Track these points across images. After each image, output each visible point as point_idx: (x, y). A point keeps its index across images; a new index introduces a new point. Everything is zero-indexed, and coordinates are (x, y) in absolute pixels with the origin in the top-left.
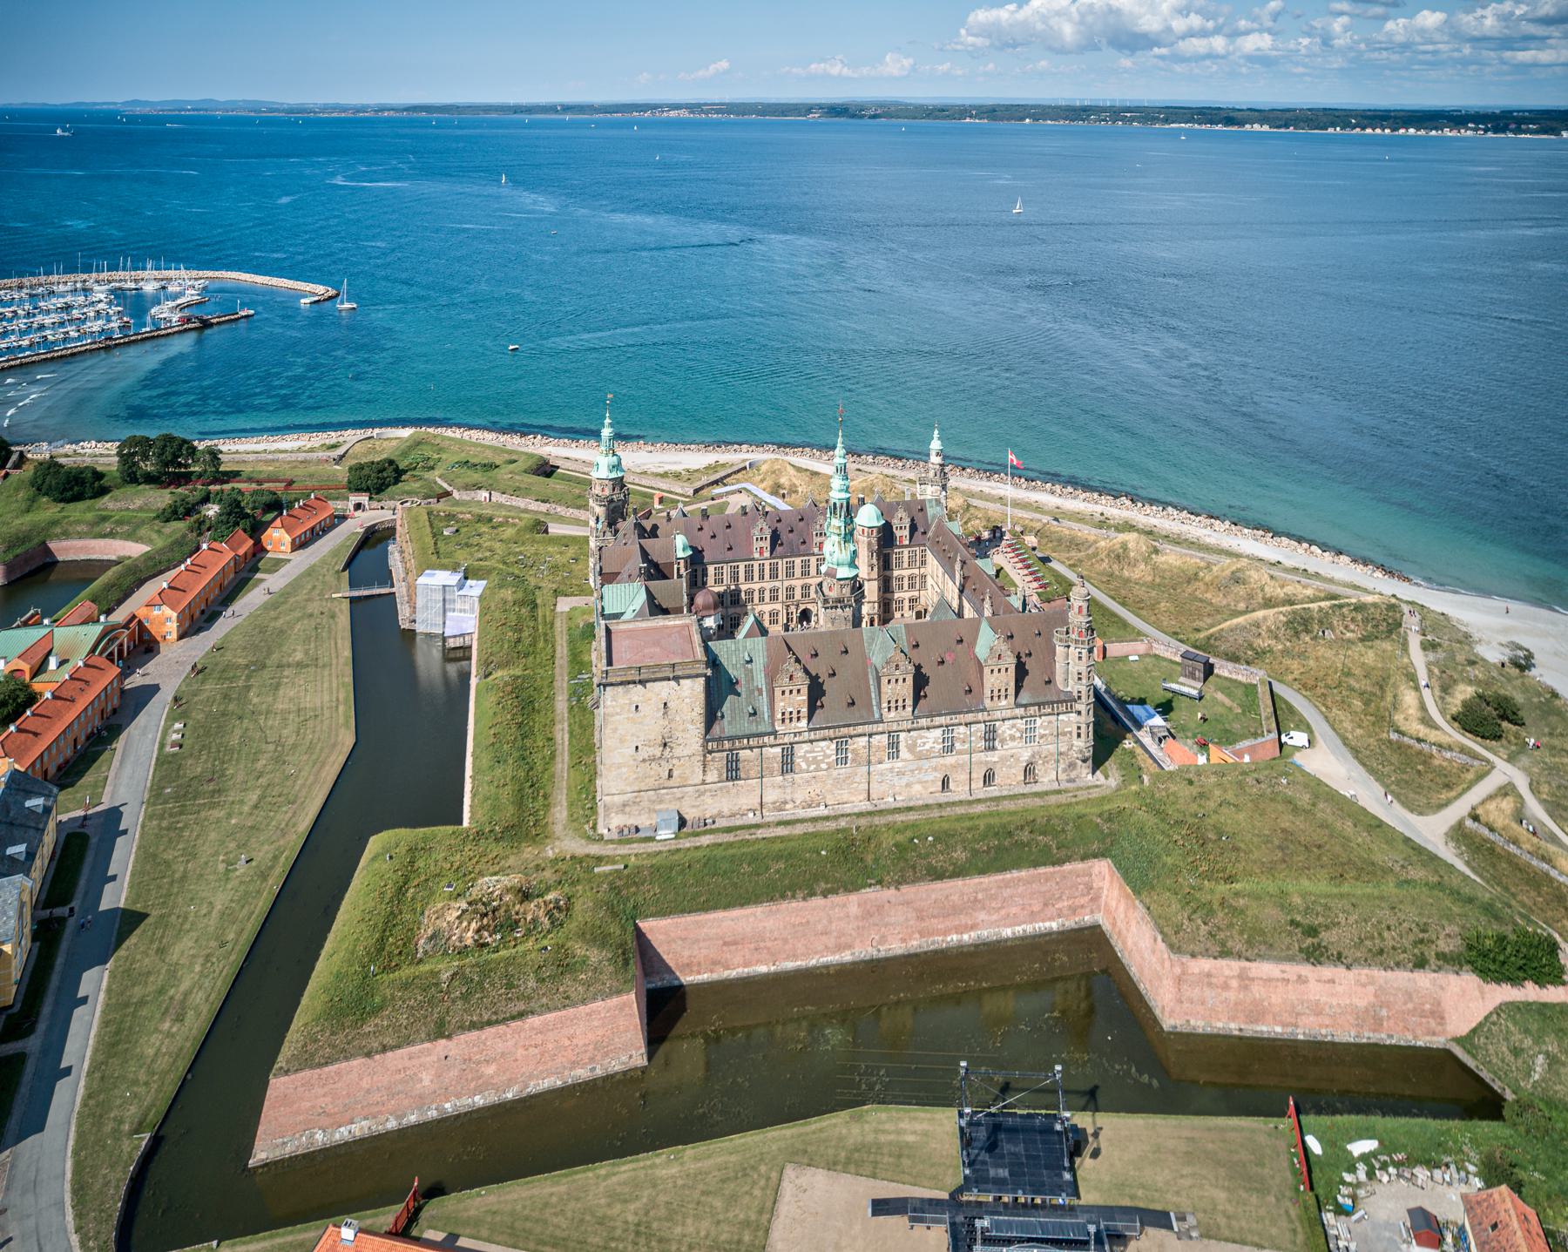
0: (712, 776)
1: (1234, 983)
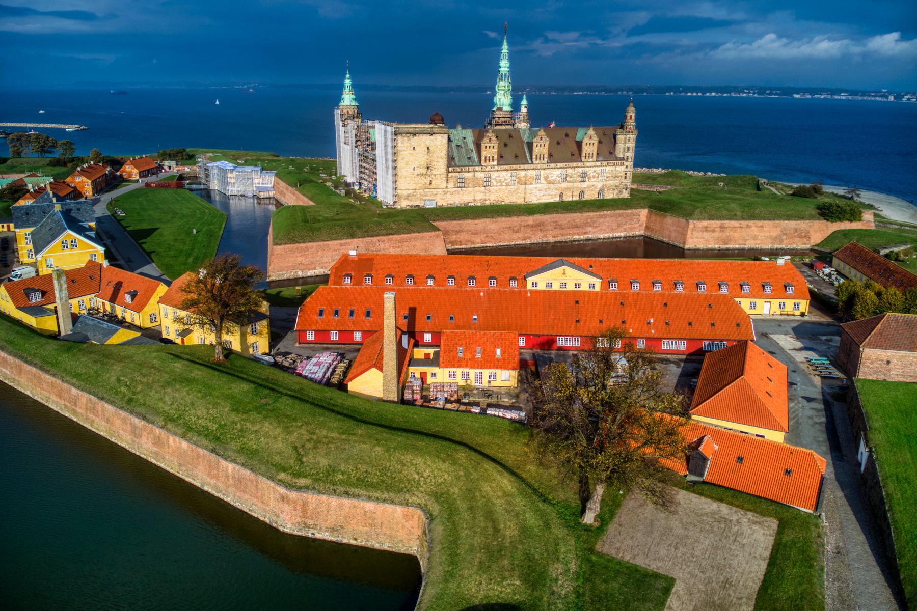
0: (451, 185)
1: (718, 229)
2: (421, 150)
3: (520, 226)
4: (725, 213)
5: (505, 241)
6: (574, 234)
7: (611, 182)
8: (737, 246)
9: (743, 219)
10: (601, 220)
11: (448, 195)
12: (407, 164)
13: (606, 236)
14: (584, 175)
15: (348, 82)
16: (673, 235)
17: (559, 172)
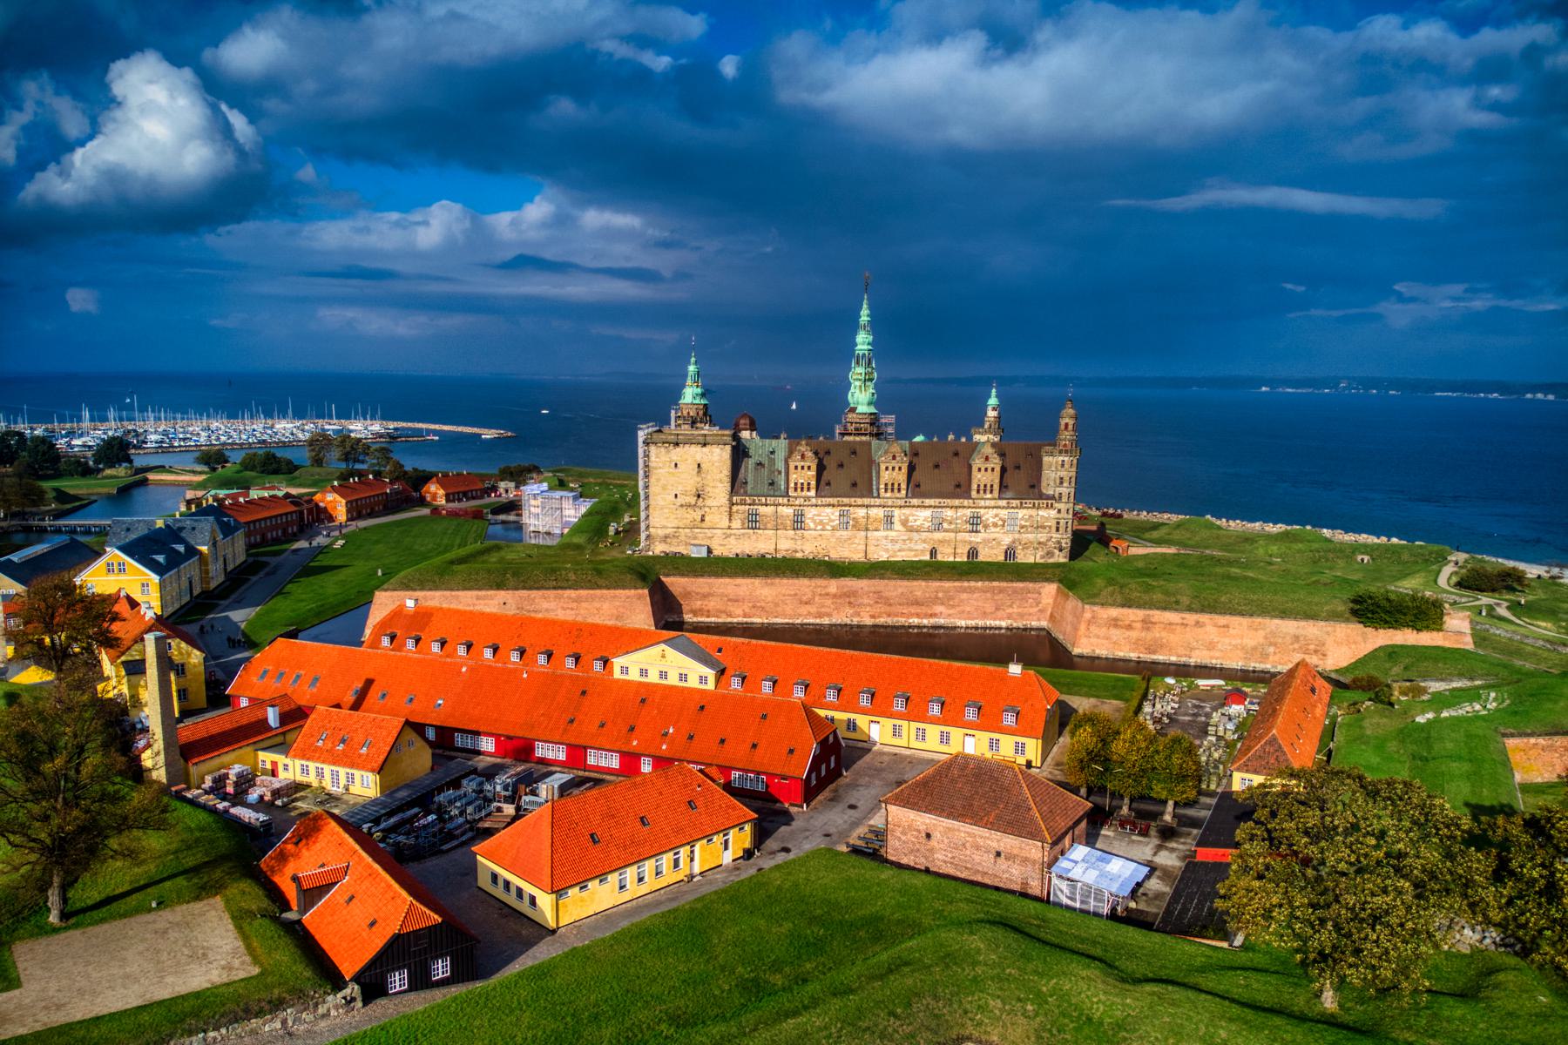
1: (1138, 625)
2: (687, 468)
3: (814, 594)
4: (1158, 596)
6: (911, 615)
8: (1173, 659)
9: (1190, 609)
10: (964, 596)
11: (732, 540)
12: (664, 488)
13: (972, 623)
14: (975, 523)
15: (692, 368)
17: (928, 513)
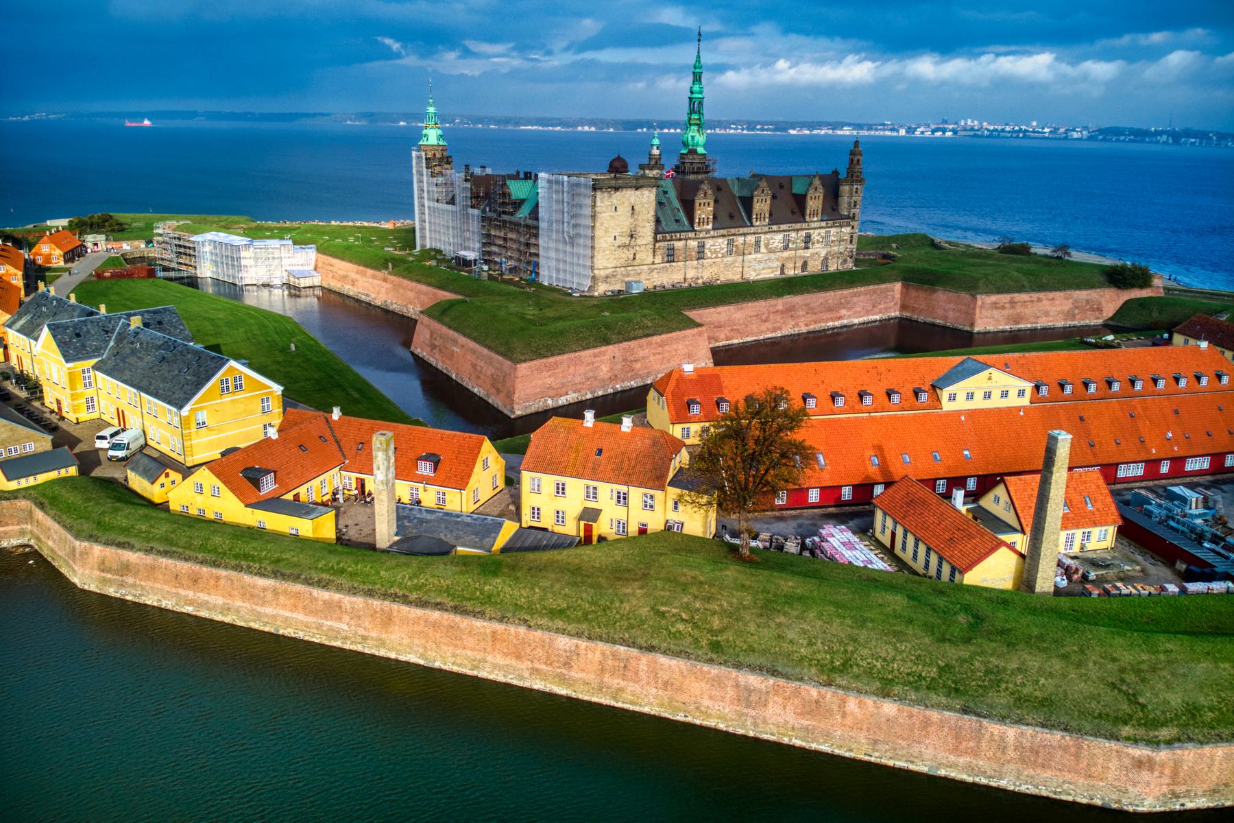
1: (1007, 305)
2: (624, 210)
5: (753, 334)
7: (836, 248)
9: (1034, 291)
10: (855, 299)
11: (655, 274)
12: (606, 232)
13: (861, 320)
16: (951, 314)
17: (780, 236)
